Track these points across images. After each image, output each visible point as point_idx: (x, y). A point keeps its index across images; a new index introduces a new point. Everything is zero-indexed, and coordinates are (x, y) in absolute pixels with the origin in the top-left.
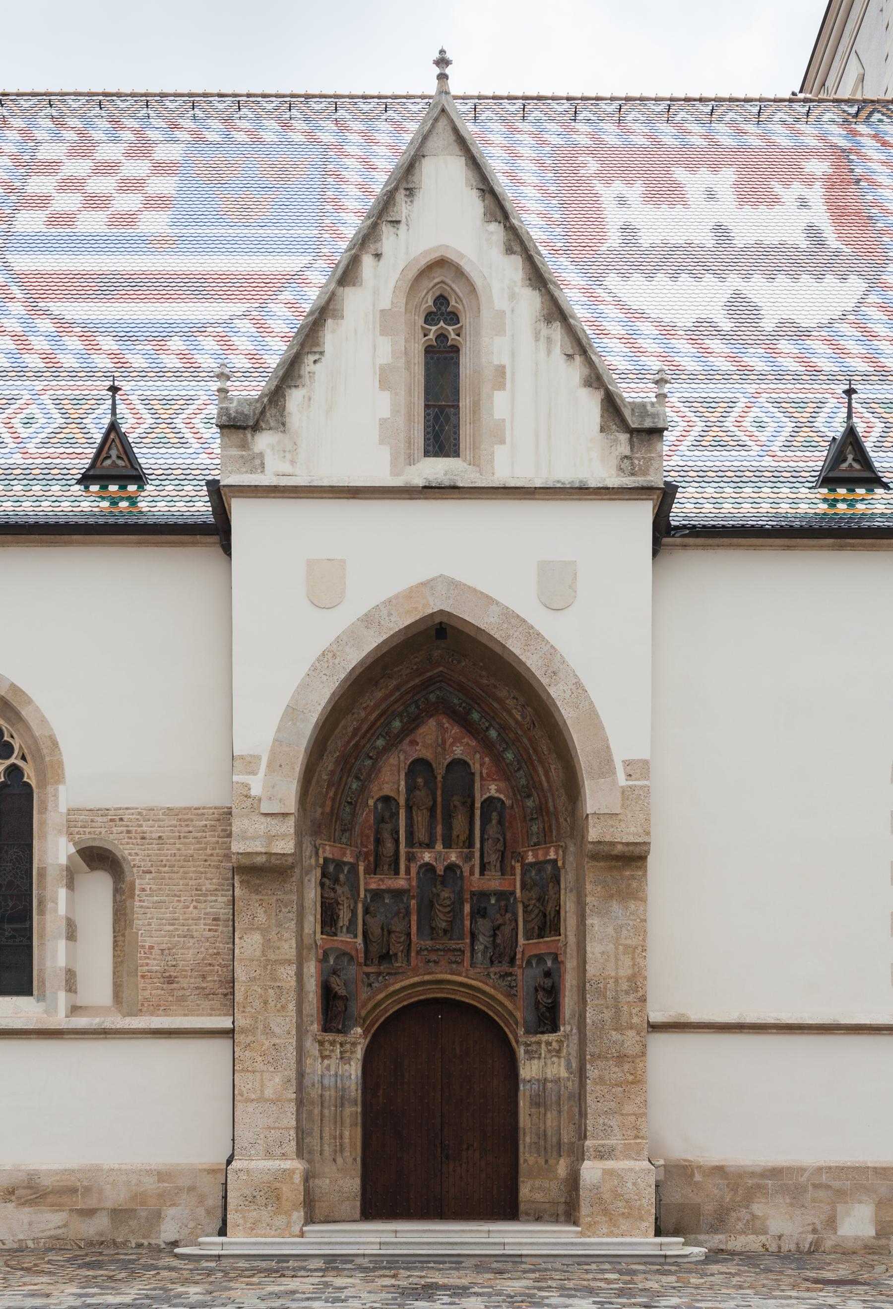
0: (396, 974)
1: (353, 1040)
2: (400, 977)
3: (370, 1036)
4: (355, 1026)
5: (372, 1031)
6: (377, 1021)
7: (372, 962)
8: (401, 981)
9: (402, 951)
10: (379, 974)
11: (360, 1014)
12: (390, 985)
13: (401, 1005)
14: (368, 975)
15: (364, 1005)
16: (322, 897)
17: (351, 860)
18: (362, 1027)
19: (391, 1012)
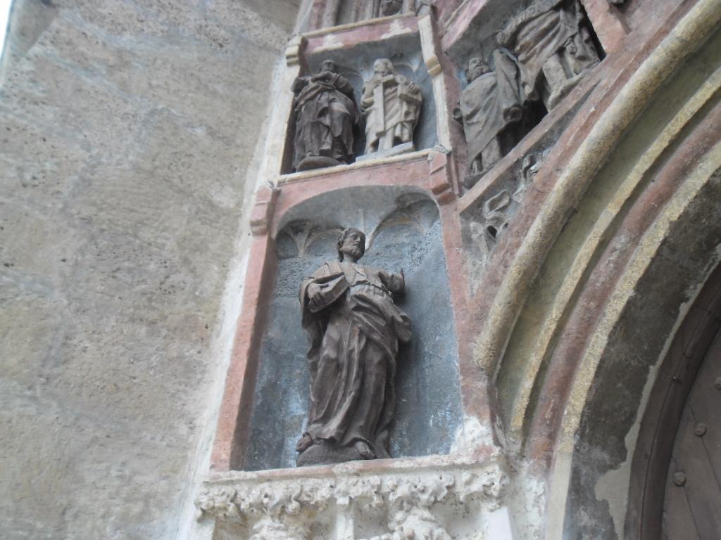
0: (562, 123)
1: (430, 481)
2: (580, 119)
3: (566, 445)
4: (457, 420)
5: (571, 422)
6: (573, 359)
7: (481, 168)
8: (586, 128)
9: (560, 52)
10: (511, 178)
11: (466, 355)
12: (550, 179)
13: (659, 231)
14: (474, 211)
15: (481, 317)
16: (295, 105)
17: (408, 30)
18: (498, 411)
19: (624, 290)
